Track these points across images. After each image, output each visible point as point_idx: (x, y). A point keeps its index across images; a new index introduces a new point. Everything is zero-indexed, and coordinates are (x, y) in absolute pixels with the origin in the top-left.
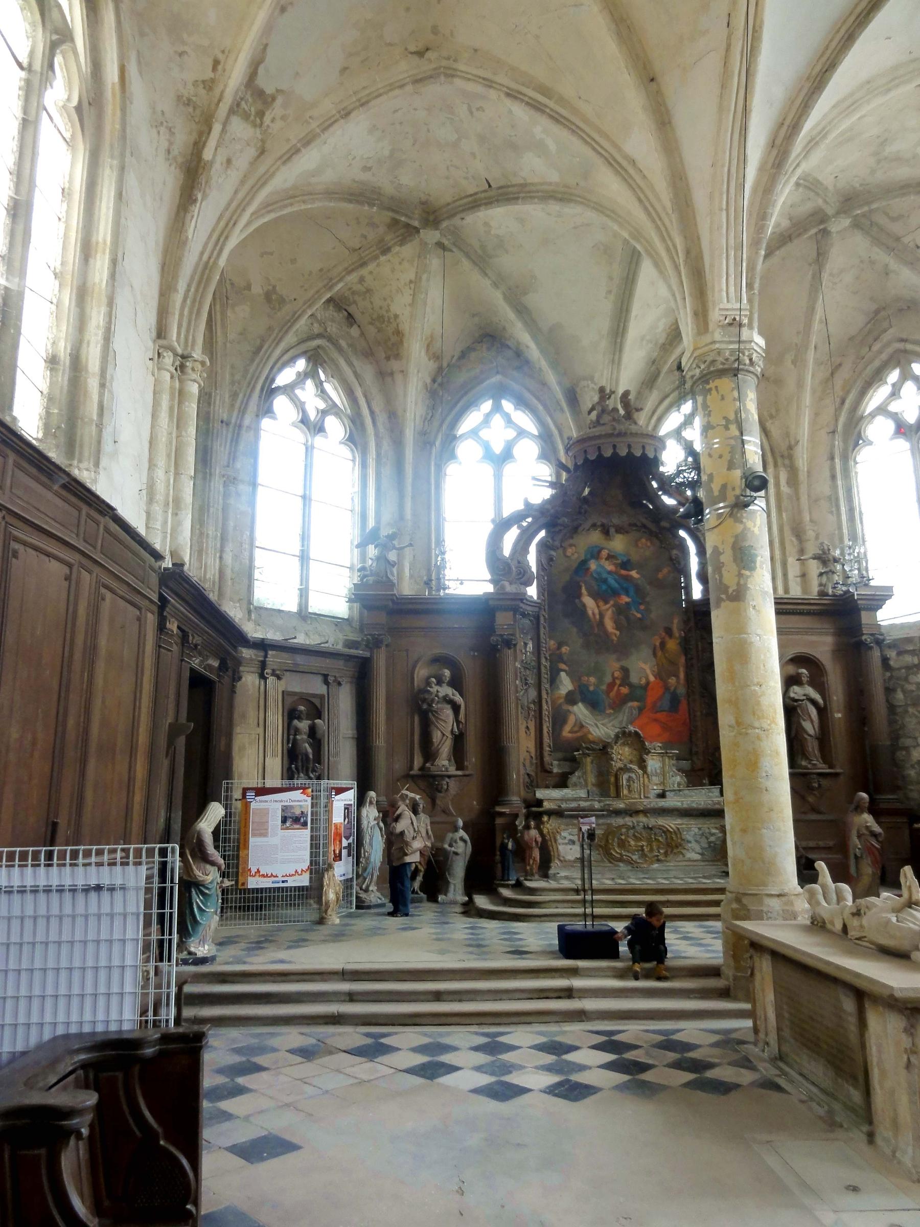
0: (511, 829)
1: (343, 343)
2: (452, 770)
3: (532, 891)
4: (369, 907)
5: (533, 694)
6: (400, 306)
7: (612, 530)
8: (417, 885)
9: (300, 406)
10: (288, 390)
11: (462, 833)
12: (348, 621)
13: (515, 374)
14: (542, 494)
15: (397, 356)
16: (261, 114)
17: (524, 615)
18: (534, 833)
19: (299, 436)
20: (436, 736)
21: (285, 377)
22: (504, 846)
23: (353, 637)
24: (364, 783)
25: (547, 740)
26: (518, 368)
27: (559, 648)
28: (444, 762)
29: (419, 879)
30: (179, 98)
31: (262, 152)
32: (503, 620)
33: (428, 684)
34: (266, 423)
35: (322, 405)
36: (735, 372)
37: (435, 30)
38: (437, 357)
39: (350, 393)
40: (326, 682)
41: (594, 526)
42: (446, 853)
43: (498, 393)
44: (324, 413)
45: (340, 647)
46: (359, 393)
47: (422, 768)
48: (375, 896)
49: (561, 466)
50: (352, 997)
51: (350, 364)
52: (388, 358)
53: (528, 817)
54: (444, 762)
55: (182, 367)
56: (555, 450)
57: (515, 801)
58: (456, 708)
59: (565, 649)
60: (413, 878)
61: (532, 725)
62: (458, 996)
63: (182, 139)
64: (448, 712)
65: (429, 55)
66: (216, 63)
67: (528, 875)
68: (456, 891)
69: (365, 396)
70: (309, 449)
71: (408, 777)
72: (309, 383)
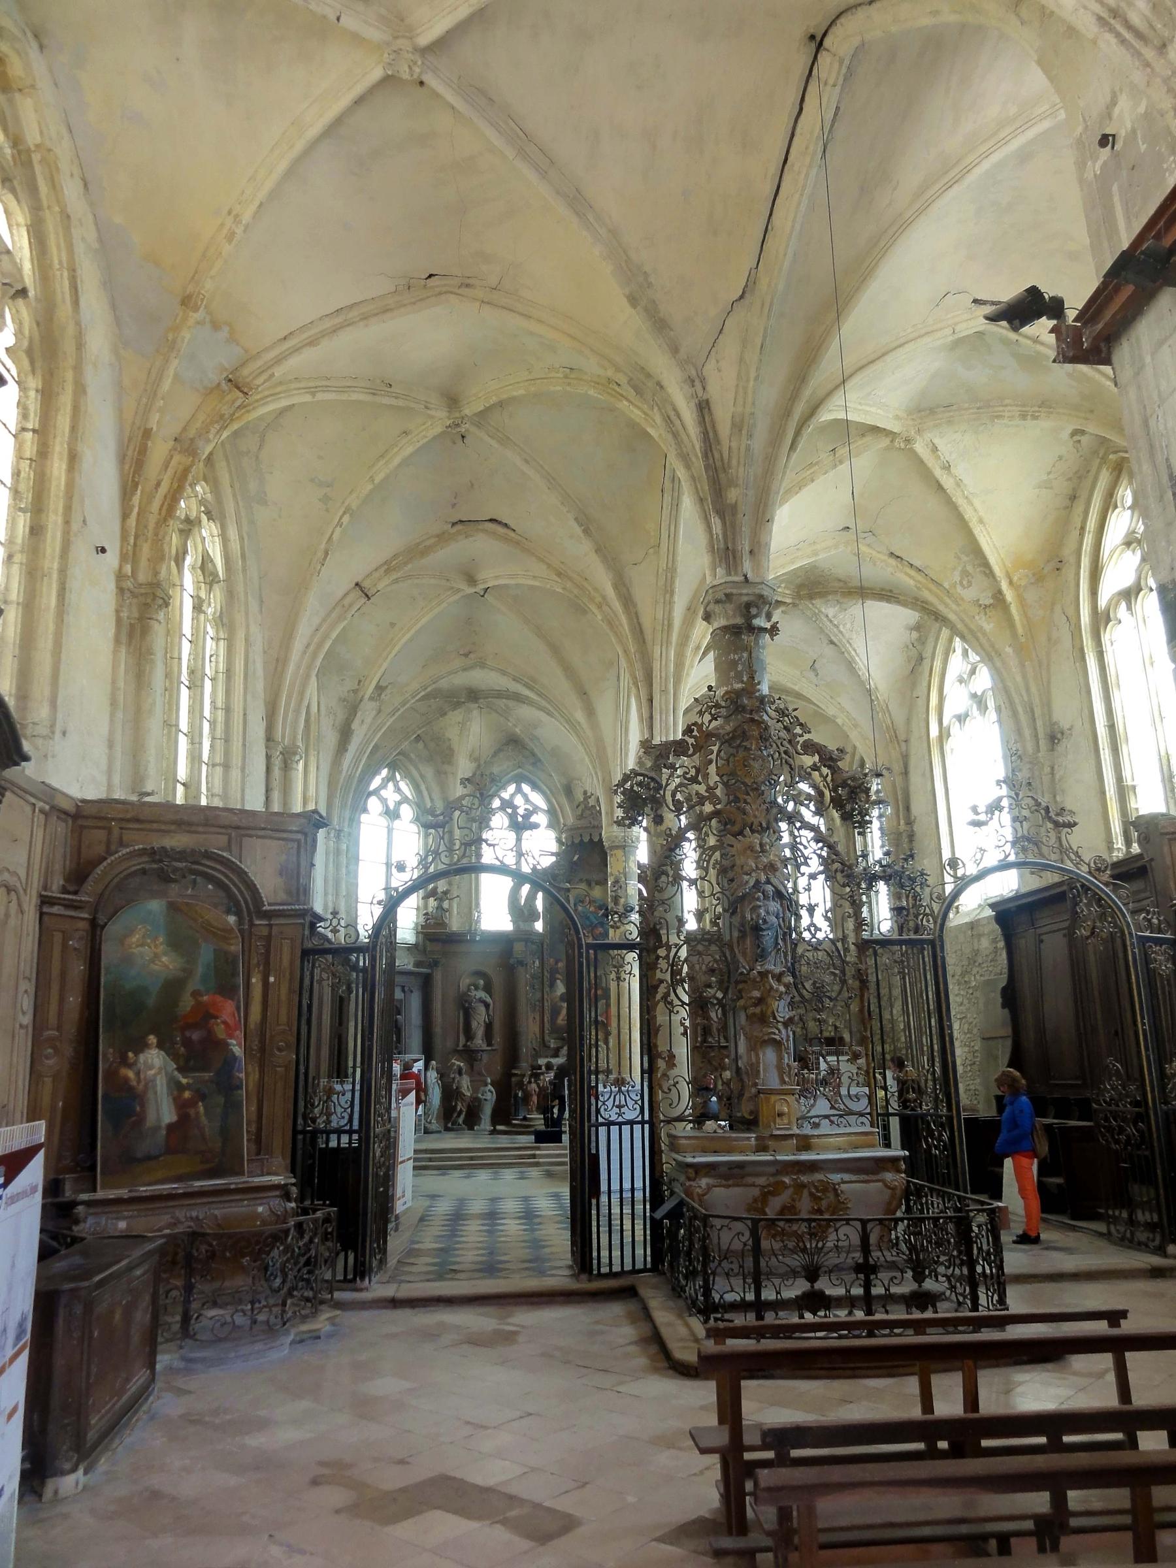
0: (521, 1085)
1: (413, 756)
2: (485, 1047)
3: (531, 1119)
4: (432, 1133)
5: (538, 995)
6: (452, 733)
7: (593, 884)
8: (461, 1120)
9: (384, 801)
10: (376, 792)
11: (490, 1087)
12: (416, 946)
13: (531, 768)
14: (547, 862)
15: (450, 763)
16: (380, 695)
17: (533, 943)
18: (534, 1086)
19: (383, 821)
20: (474, 1024)
21: (376, 782)
22: (516, 1095)
23: (420, 958)
24: (428, 1056)
25: (547, 1025)
26: (534, 764)
27: (556, 963)
28: (479, 1041)
29: (462, 1117)
30: (340, 699)
31: (379, 711)
32: (518, 948)
33: (469, 990)
34: (364, 817)
35: (398, 797)
36: (624, 847)
37: (474, 644)
38: (477, 760)
39: (416, 787)
40: (403, 991)
41: (581, 880)
42: (479, 1100)
43: (519, 780)
44: (399, 803)
45: (410, 967)
46: (423, 787)
47: (465, 1046)
48: (435, 1126)
49: (559, 841)
50: (430, 1160)
51: (418, 769)
52: (443, 763)
53: (531, 1076)
54: (479, 1041)
55: (338, 837)
56: (558, 822)
57: (524, 1066)
58: (487, 1006)
59: (560, 965)
60: (459, 1116)
61: (538, 1018)
62: (482, 1158)
63: (341, 716)
64: (482, 1009)
65: (471, 656)
66: (360, 681)
67: (530, 1111)
68: (486, 1123)
69: (427, 789)
70: (390, 831)
71: (456, 1052)
72: (391, 785)
